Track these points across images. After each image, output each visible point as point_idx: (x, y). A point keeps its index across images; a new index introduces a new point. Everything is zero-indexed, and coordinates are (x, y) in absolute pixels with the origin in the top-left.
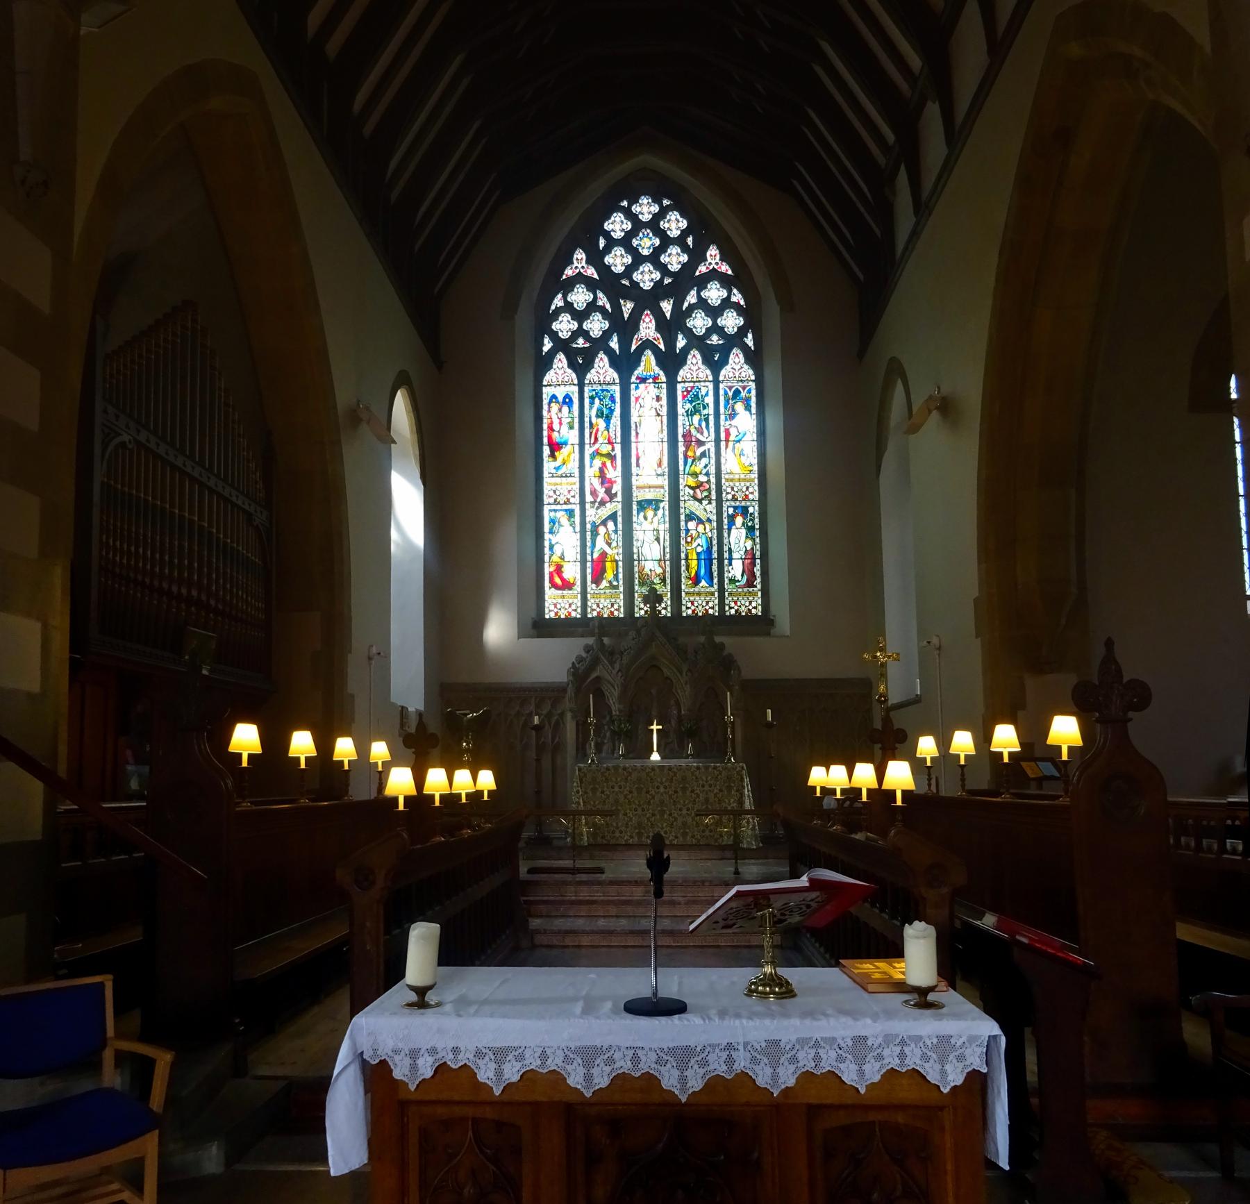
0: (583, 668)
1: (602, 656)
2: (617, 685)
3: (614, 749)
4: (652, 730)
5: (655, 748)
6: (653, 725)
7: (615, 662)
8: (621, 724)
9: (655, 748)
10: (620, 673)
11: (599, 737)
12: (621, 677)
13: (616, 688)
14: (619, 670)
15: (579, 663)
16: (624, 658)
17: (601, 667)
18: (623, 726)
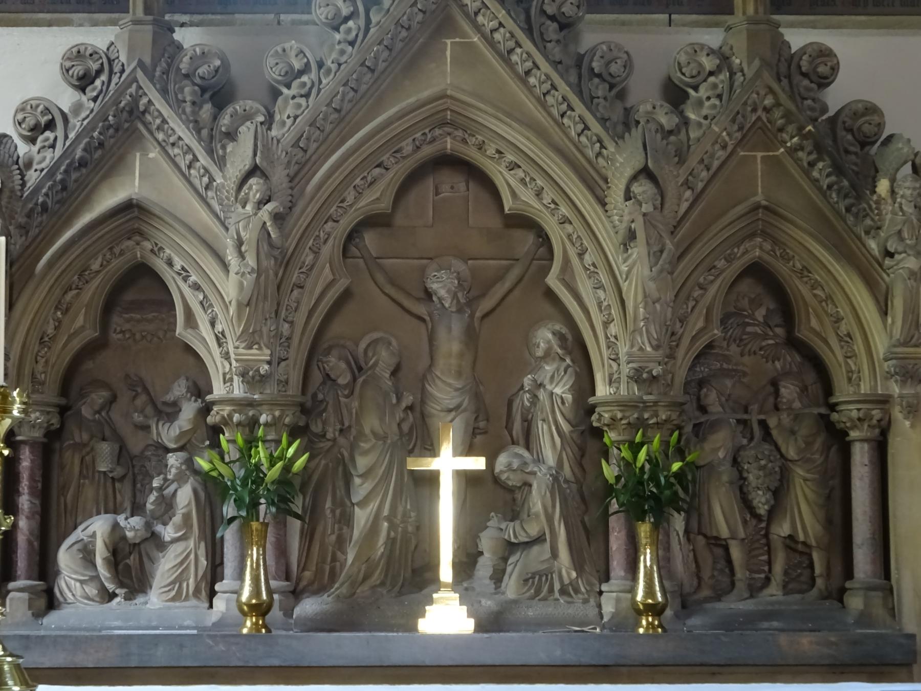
0: (50, 157)
1: (160, 104)
2: (240, 243)
3: (215, 572)
4: (432, 479)
5: (446, 573)
6: (432, 450)
7: (231, 135)
8: (251, 442)
9: (446, 573)
10: (255, 182)
11: (137, 509)
12: (261, 204)
13: (231, 257)
14: (254, 171)
15: (32, 140)
16: (285, 111)
17: (154, 154)
18: (261, 454)
